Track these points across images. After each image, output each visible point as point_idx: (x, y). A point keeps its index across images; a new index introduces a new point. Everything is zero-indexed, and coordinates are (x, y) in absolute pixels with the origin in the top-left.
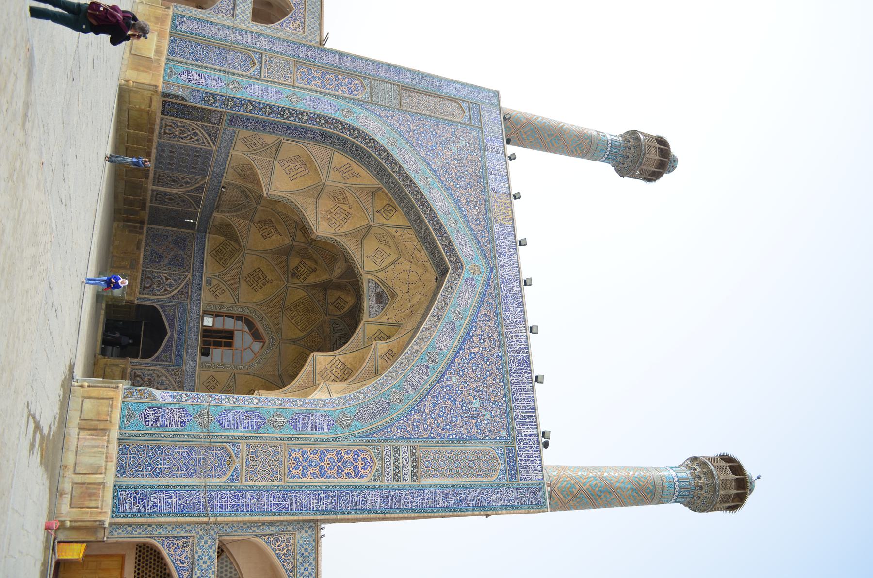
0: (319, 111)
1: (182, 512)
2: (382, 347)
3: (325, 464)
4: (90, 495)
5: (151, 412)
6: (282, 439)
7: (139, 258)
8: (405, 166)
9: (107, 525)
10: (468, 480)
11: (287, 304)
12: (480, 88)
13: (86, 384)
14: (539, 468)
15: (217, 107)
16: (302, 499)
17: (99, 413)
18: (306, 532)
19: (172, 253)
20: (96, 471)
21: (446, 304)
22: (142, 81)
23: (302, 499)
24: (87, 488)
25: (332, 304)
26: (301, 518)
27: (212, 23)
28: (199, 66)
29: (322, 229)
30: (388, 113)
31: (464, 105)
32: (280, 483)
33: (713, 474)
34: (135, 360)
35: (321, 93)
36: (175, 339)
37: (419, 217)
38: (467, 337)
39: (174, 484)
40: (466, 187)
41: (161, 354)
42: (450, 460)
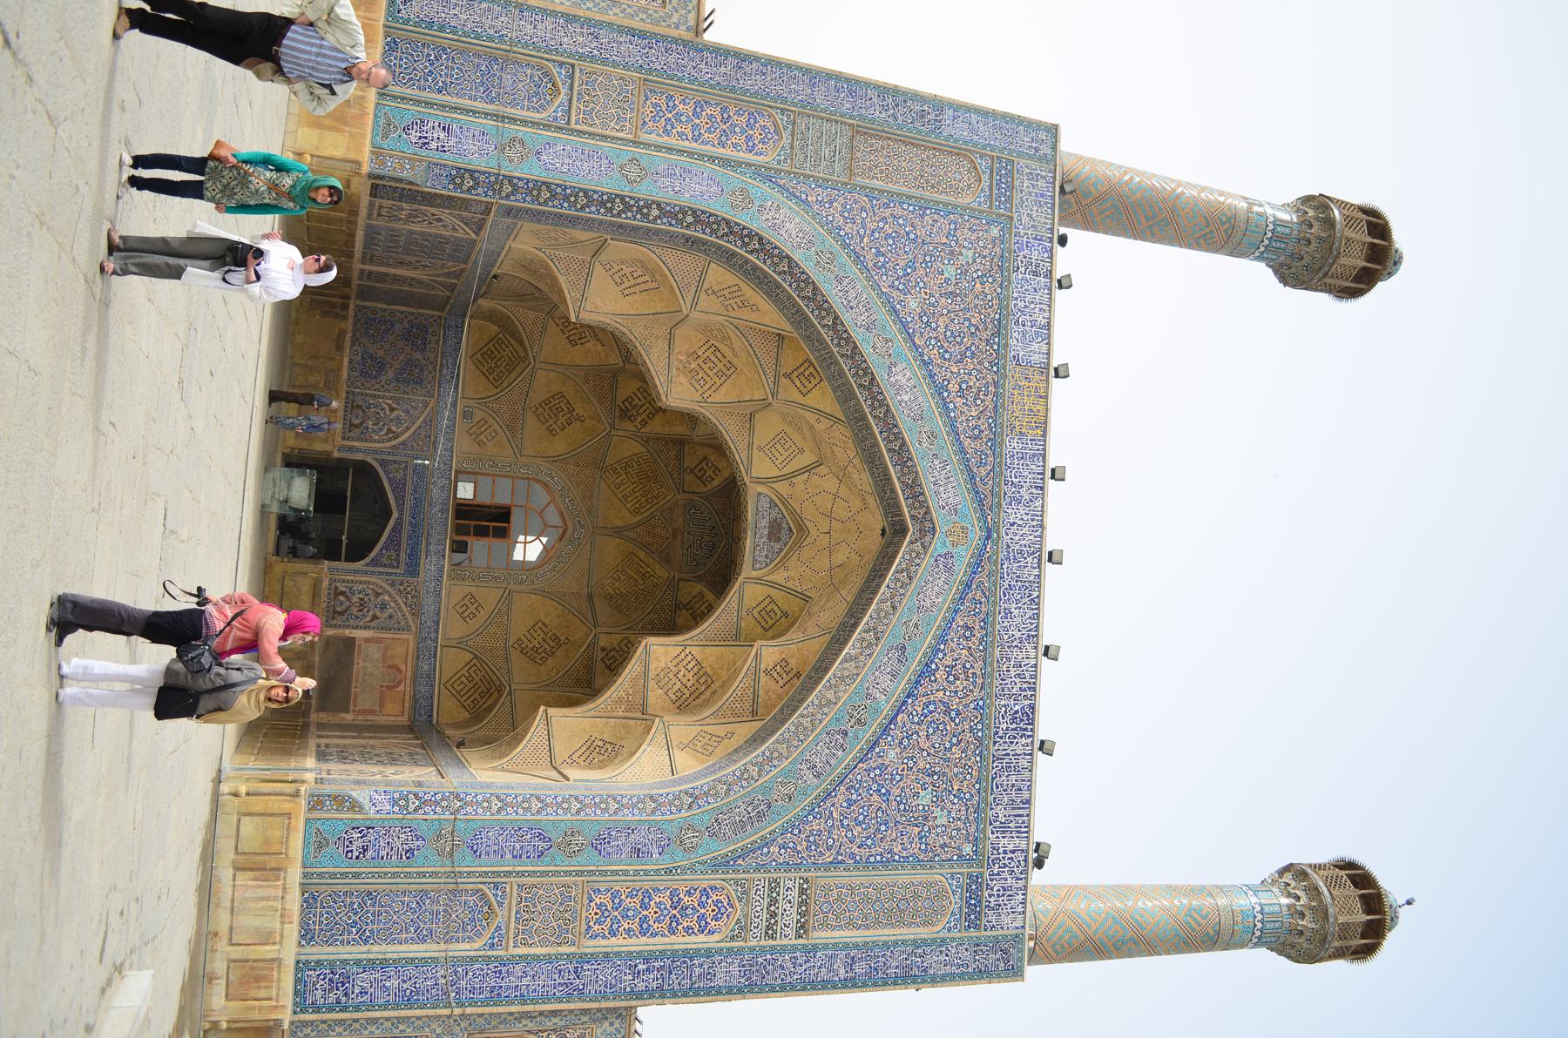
0: (685, 200)
2: (769, 653)
4: (258, 979)
5: (356, 836)
6: (579, 873)
7: (340, 369)
8: (846, 317)
9: (286, 1026)
10: (893, 931)
11: (609, 461)
12: (1019, 121)
13: (243, 789)
14: (1020, 909)
15: (480, 195)
16: (606, 974)
17: (266, 841)
18: (612, 1024)
19: (402, 357)
20: (266, 938)
21: (894, 608)
22: (328, 152)
23: (606, 974)
24: (253, 968)
25: (692, 471)
26: (604, 1005)
28: (443, 107)
29: (677, 392)
30: (823, 194)
31: (982, 164)
32: (573, 949)
33: (1326, 913)
34: (336, 564)
35: (691, 154)
36: (406, 525)
37: (864, 418)
38: (926, 671)
39: (395, 956)
42: (866, 899)
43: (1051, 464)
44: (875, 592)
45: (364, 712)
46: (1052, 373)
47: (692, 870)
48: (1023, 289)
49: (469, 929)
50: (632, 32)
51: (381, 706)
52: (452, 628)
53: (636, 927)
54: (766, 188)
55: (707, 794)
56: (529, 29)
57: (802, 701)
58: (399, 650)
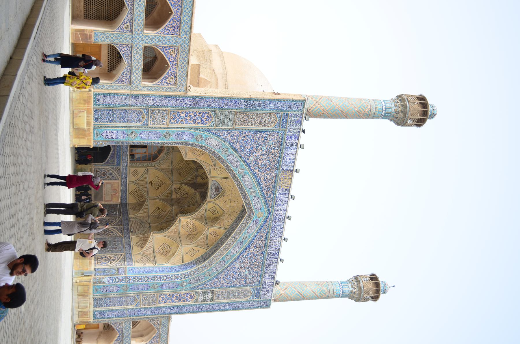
1: (119, 317)
2: (211, 229)
3: (174, 298)
8: (230, 165)
13: (78, 281)
15: (124, 144)
17: (84, 290)
20: (86, 307)
23: (163, 310)
27: (118, 95)
29: (188, 156)
35: (184, 128)
36: (115, 152)
38: (249, 246)
40: (266, 170)
41: (109, 160)
43: (292, 193)
44: (237, 227)
45: (107, 201)
46: (295, 170)
47: (185, 290)
48: (287, 150)
49: (131, 303)
50: (166, 96)
51: (112, 199)
52: (131, 178)
53: (171, 301)
54: (207, 134)
55: (188, 275)
56: (135, 101)
57: (215, 251)
58: (116, 185)
